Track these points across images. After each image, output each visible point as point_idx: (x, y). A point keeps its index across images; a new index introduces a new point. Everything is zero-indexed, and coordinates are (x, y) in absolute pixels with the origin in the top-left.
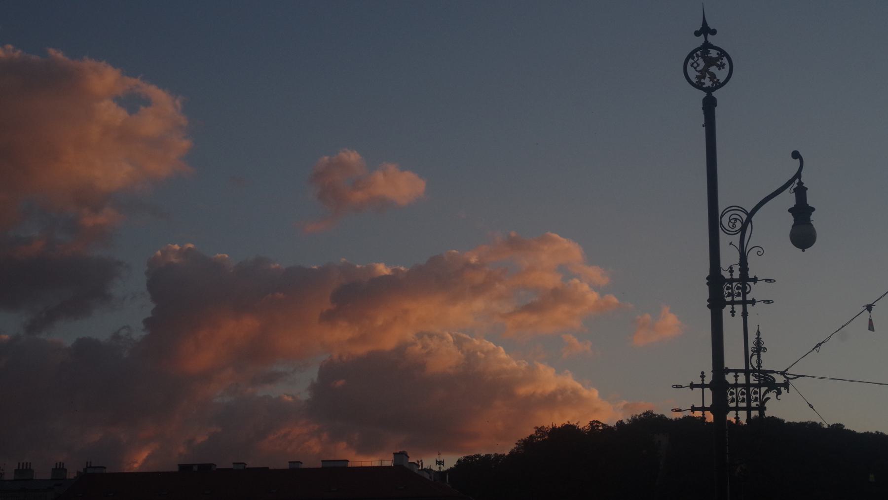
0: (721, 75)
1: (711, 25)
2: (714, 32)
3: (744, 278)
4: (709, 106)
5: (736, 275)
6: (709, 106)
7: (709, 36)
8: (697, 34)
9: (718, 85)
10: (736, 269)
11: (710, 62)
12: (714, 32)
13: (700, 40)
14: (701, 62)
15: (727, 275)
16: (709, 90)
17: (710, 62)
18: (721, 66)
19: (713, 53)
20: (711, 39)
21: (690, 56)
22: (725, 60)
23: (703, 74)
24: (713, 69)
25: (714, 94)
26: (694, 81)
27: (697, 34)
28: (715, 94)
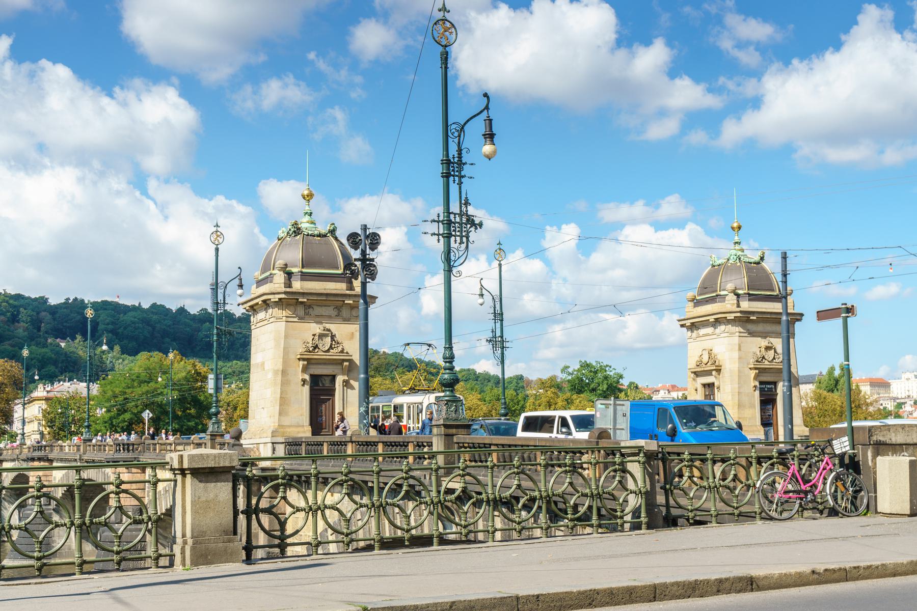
0: (221, 240)
1: (219, 225)
3: (224, 303)
4: (217, 250)
5: (222, 302)
6: (217, 250)
10: (222, 300)
11: (218, 236)
13: (215, 229)
14: (215, 237)
15: (219, 302)
17: (218, 236)
18: (221, 238)
19: (219, 233)
20: (219, 229)
24: (218, 238)
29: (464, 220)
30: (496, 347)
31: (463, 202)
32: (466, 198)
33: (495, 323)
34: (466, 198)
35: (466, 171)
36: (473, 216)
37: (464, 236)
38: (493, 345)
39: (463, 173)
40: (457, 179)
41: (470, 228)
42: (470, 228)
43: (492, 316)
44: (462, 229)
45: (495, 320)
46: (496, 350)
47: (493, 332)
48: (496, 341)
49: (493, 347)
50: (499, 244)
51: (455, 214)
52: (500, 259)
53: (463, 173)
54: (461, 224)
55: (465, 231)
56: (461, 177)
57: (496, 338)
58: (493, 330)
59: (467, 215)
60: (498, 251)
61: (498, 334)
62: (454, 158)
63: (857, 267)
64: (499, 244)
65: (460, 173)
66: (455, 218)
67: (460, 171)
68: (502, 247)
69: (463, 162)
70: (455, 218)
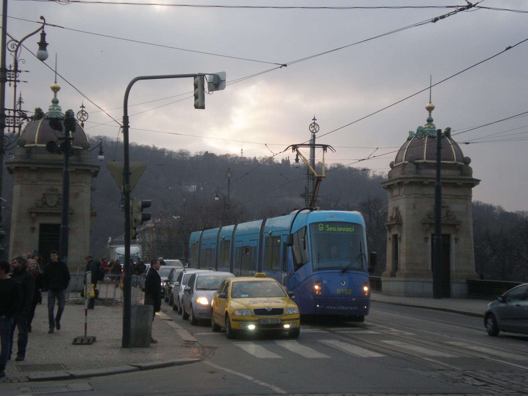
0: (85, 118)
2: (84, 107)
7: (83, 108)
8: (81, 107)
9: (85, 120)
11: (83, 114)
12: (84, 107)
13: (81, 109)
14: (81, 115)
16: (82, 121)
17: (83, 114)
18: (86, 116)
19: (84, 112)
20: (84, 109)
21: (79, 113)
22: (86, 115)
23: (81, 117)
24: (84, 116)
25: (84, 122)
26: (79, 118)
27: (81, 107)
28: (84, 122)
29: (17, 114)
31: (17, 100)
32: (20, 98)
33: (308, 182)
34: (20, 98)
35: (21, 77)
36: (26, 111)
37: (17, 127)
38: (305, 199)
39: (17, 79)
40: (13, 83)
41: (23, 120)
42: (23, 120)
44: (15, 121)
45: (308, 179)
47: (306, 189)
50: (314, 119)
51: (9, 110)
52: (314, 131)
53: (17, 79)
54: (14, 117)
55: (18, 123)
56: (15, 81)
57: (308, 194)
58: (306, 187)
59: (20, 110)
60: (313, 125)
62: (10, 67)
63: (377, 148)
64: (314, 119)
65: (15, 79)
66: (9, 112)
67: (16, 77)
68: (316, 122)
69: (19, 69)
70: (9, 112)
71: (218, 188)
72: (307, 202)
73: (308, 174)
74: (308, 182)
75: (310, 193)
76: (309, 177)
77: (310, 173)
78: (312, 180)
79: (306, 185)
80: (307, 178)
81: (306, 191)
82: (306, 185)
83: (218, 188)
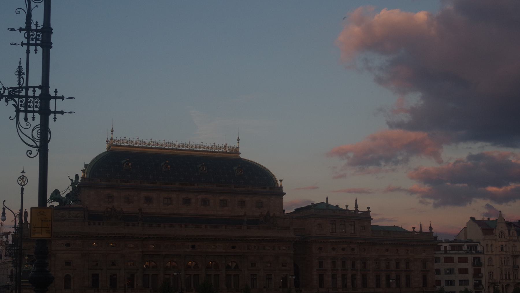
30: (26, 112)
33: (28, 52)
43: (21, 37)
45: (28, 44)
46: (26, 119)
47: (19, 73)
48: (27, 97)
49: (18, 111)
57: (27, 88)
61: (35, 79)
71: (5, 201)
72: (22, 115)
73: (28, 29)
74: (28, 52)
75: (34, 88)
76: (28, 38)
77: (33, 27)
78: (40, 49)
79: (20, 63)
80: (25, 41)
81: (19, 81)
82: (20, 63)
83: (5, 201)
